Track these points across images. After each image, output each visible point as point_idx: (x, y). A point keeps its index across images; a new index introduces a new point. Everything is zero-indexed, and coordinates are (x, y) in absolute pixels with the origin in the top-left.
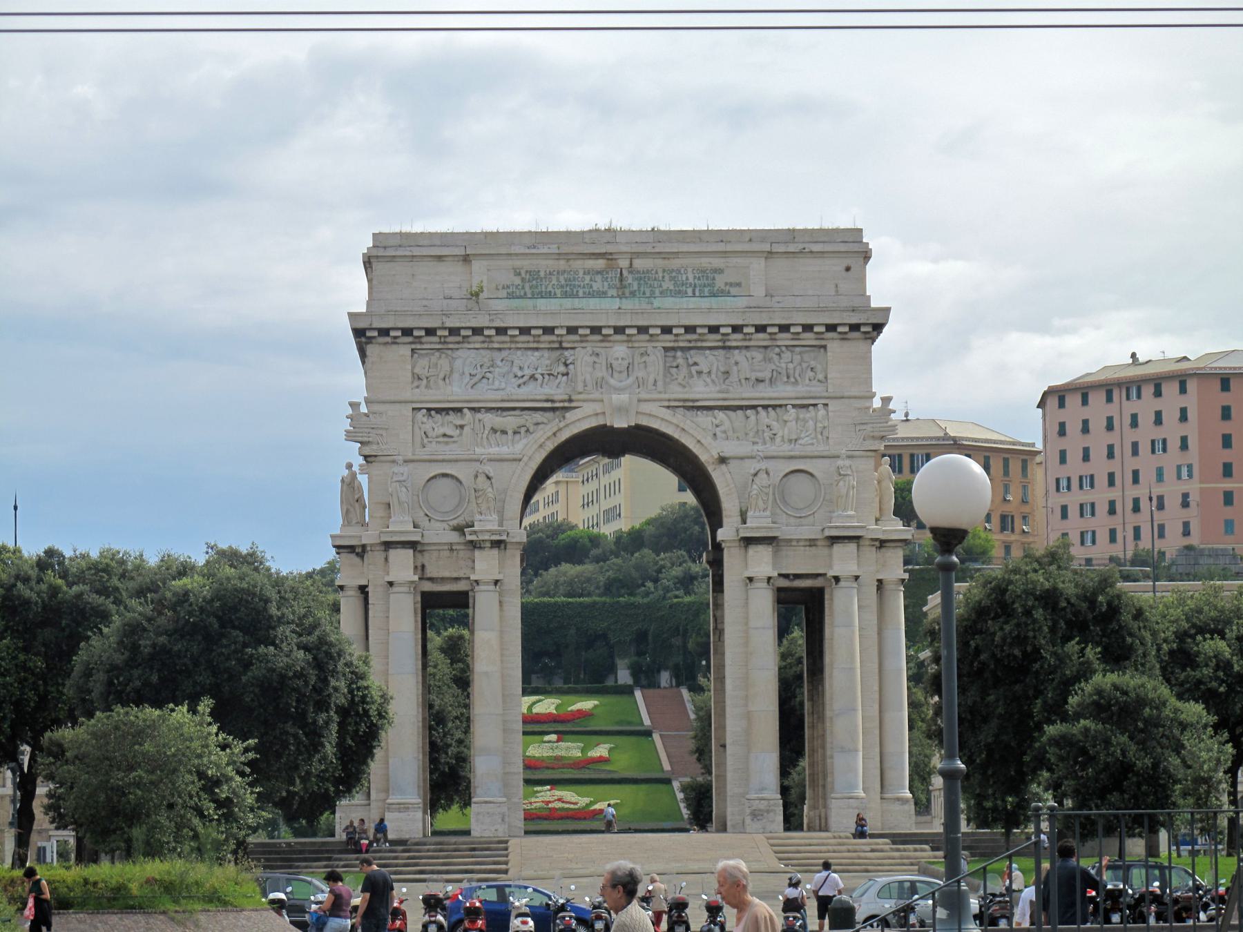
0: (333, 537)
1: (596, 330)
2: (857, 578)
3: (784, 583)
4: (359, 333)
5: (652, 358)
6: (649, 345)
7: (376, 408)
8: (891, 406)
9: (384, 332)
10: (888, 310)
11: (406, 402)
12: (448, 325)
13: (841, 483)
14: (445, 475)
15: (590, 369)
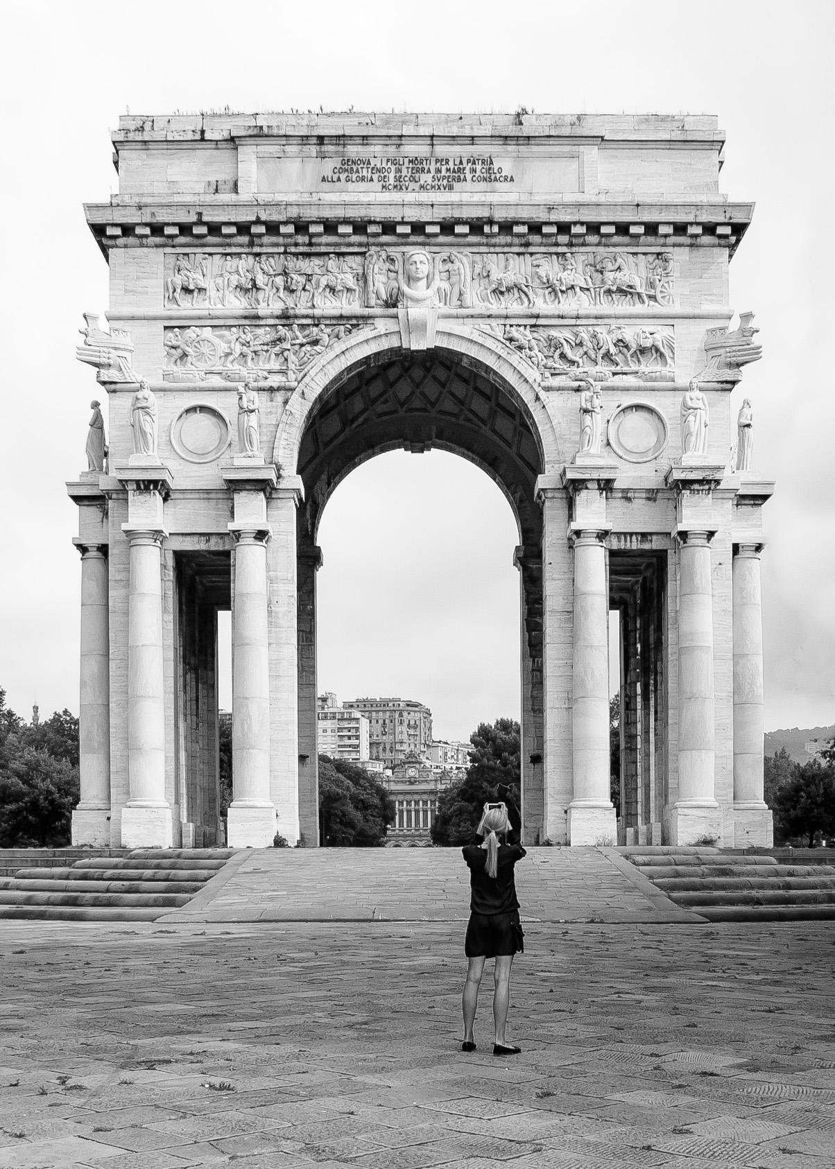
0: (68, 485)
1: (389, 227)
2: (711, 534)
3: (615, 544)
4: (99, 230)
5: (457, 264)
6: (454, 250)
7: (117, 324)
8: (753, 324)
9: (127, 230)
10: (749, 207)
11: (155, 319)
12: (205, 219)
13: (691, 418)
14: (203, 409)
15: (383, 279)
